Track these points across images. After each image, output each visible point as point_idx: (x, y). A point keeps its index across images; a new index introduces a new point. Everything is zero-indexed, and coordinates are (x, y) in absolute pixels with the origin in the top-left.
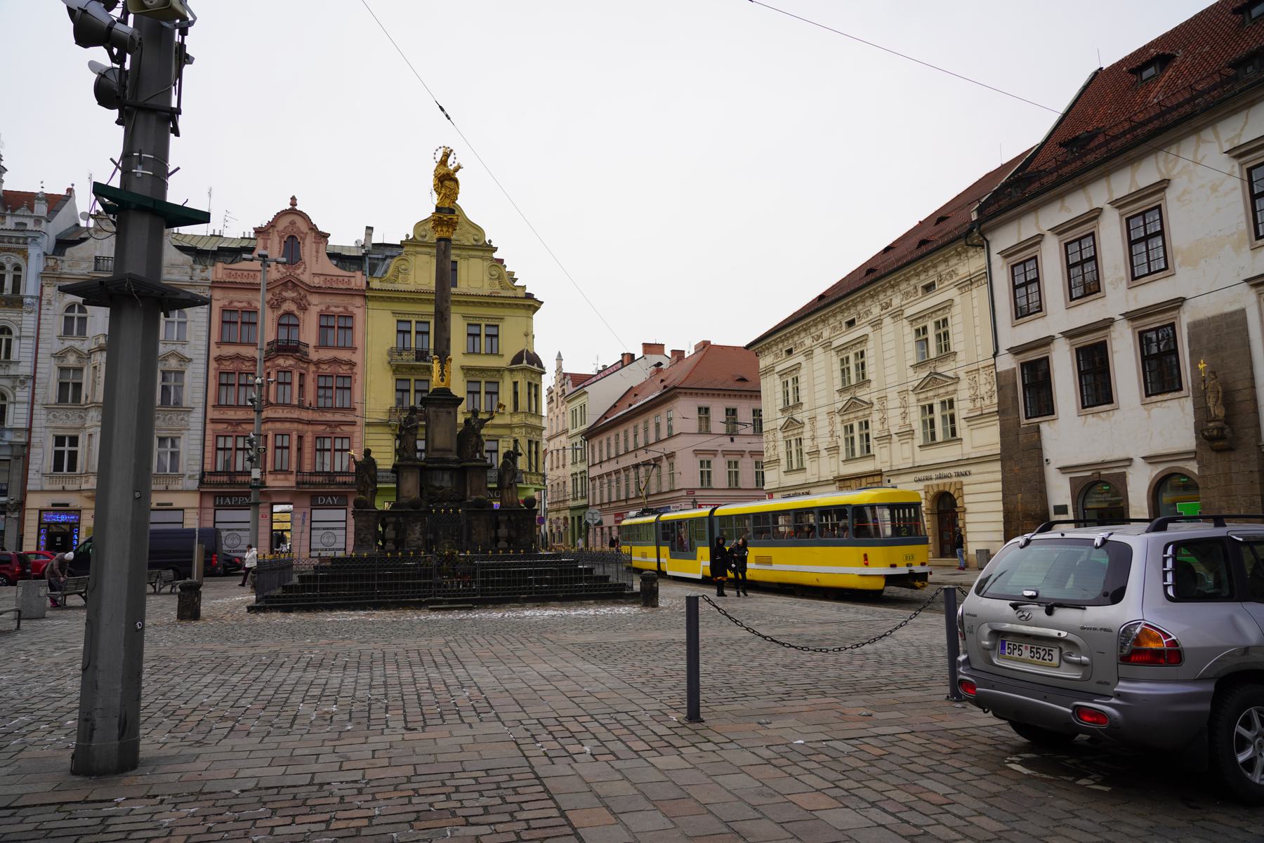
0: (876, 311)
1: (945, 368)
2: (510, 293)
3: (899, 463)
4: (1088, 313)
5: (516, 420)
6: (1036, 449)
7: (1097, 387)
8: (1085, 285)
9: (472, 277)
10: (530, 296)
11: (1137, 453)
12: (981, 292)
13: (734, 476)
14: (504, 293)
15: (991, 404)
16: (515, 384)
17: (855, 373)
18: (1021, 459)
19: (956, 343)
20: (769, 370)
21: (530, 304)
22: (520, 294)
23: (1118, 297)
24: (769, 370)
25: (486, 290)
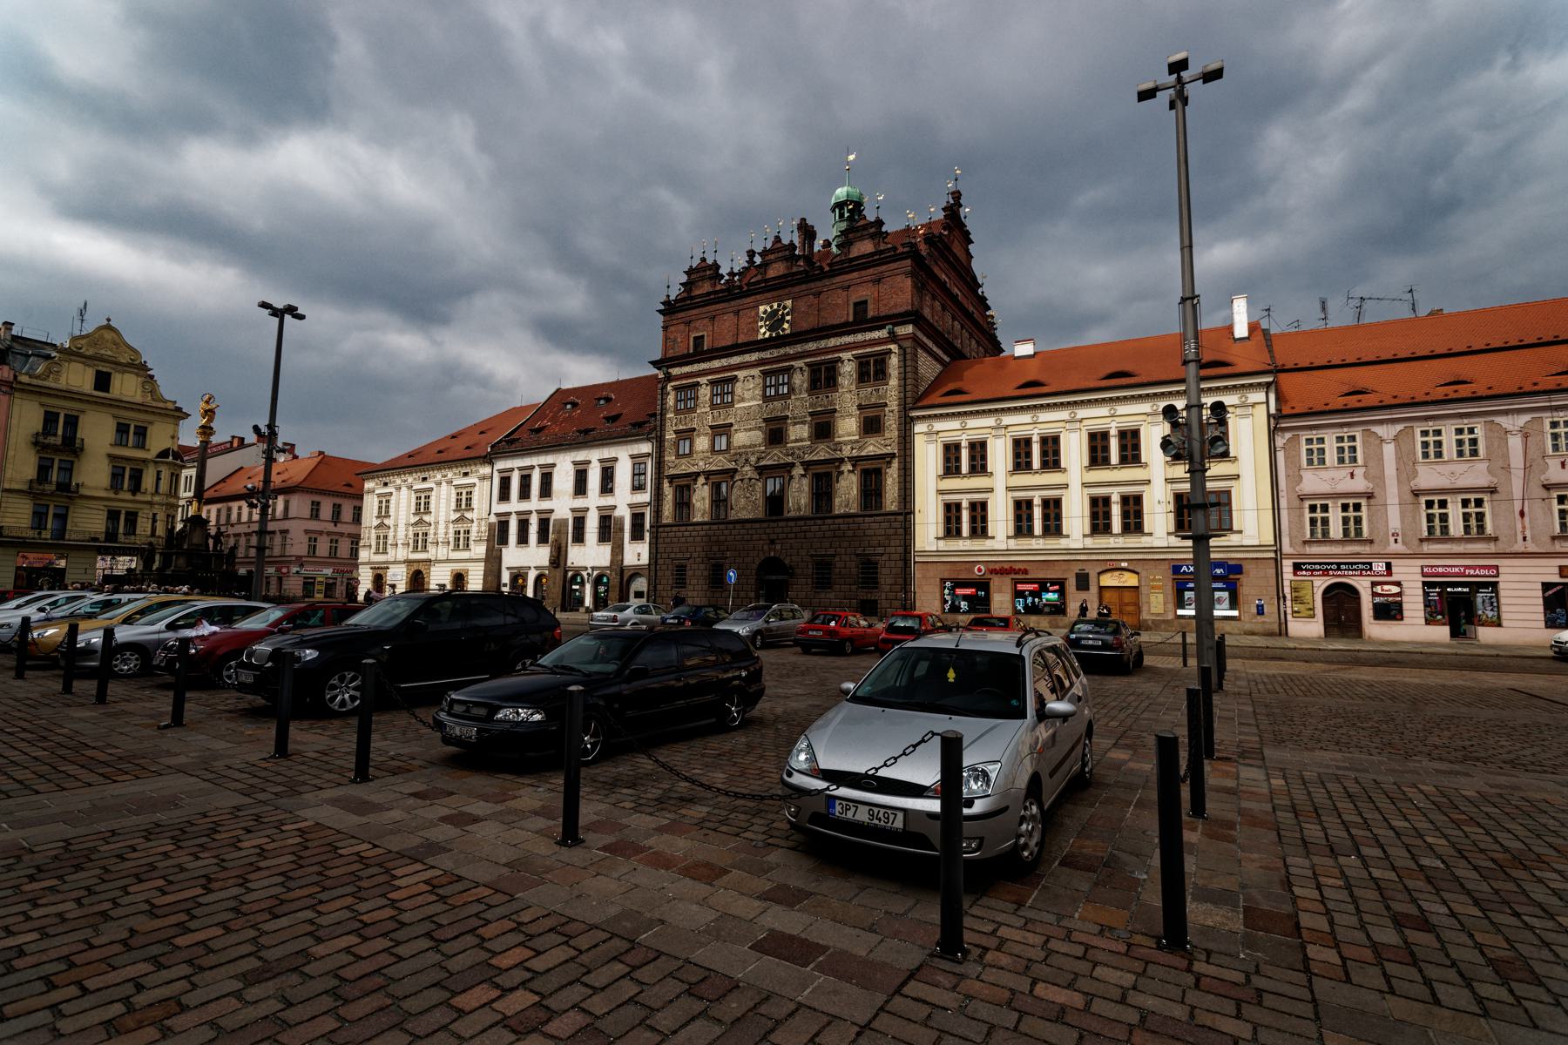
0: (439, 476)
1: (468, 515)
2: (161, 405)
3: (440, 557)
4: (524, 506)
5: (157, 499)
6: (500, 559)
7: (523, 539)
8: (525, 494)
9: (125, 387)
10: (179, 409)
11: (532, 565)
12: (487, 483)
13: (333, 552)
14: (154, 404)
15: (485, 535)
16: (159, 473)
17: (423, 506)
18: (493, 561)
19: (475, 503)
20: (372, 491)
21: (178, 414)
22: (170, 406)
23: (535, 503)
24: (372, 491)
25: (138, 398)
